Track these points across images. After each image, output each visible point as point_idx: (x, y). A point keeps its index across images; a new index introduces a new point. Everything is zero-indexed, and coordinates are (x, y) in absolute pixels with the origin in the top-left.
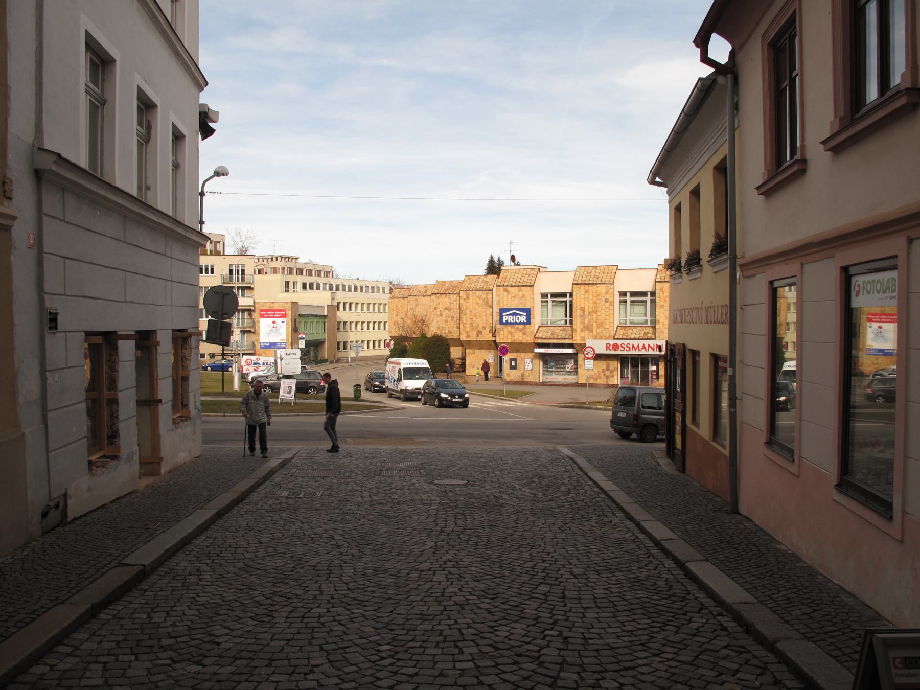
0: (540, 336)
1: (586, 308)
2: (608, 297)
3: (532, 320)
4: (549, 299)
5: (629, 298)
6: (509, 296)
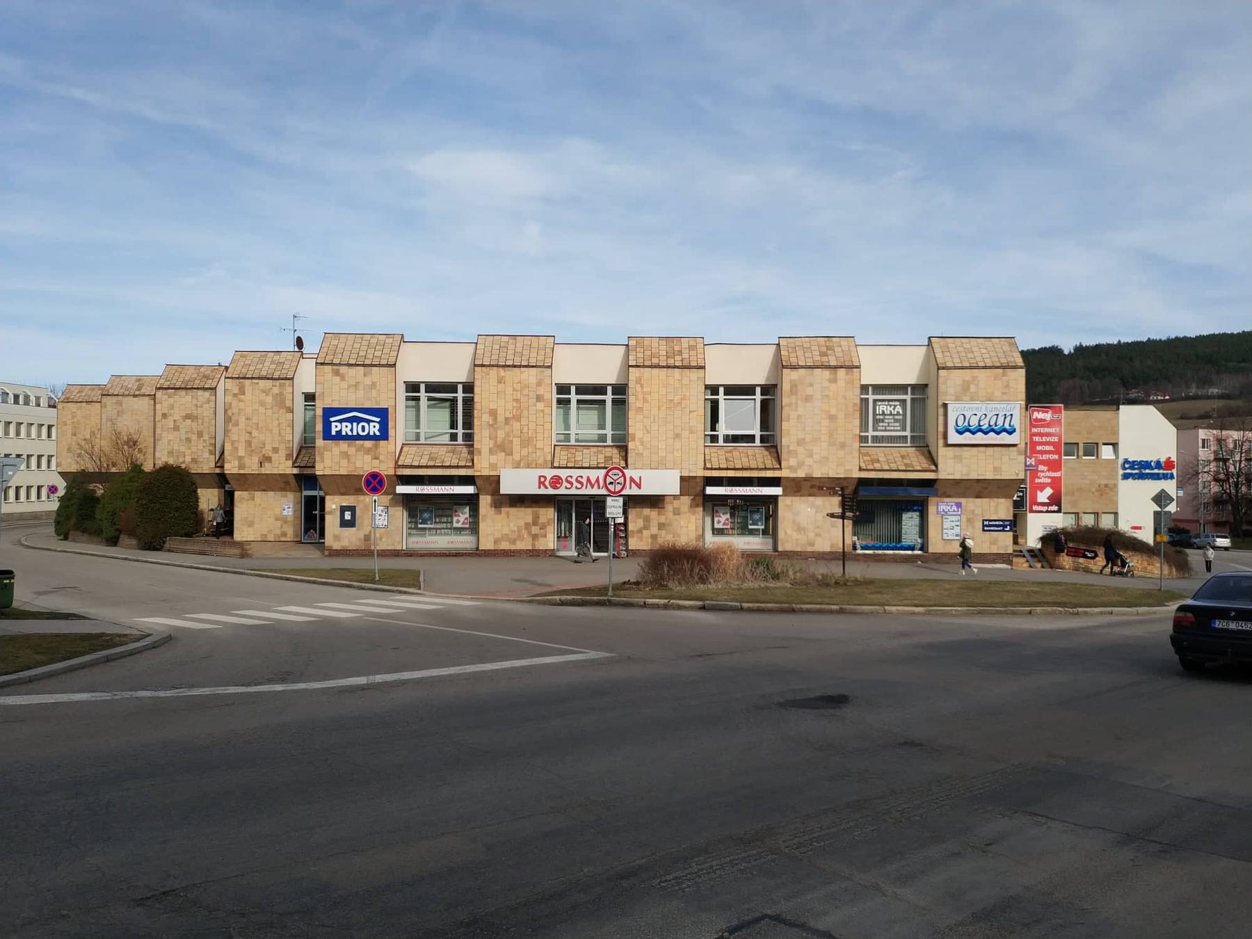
0: (408, 462)
1: (500, 412)
2: (541, 391)
3: (391, 432)
4: (423, 394)
5: (574, 397)
6: (344, 385)
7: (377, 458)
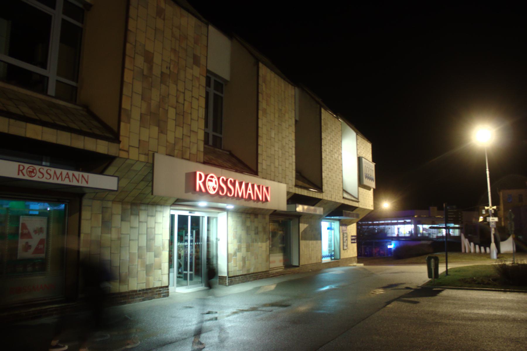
1: (157, 59)
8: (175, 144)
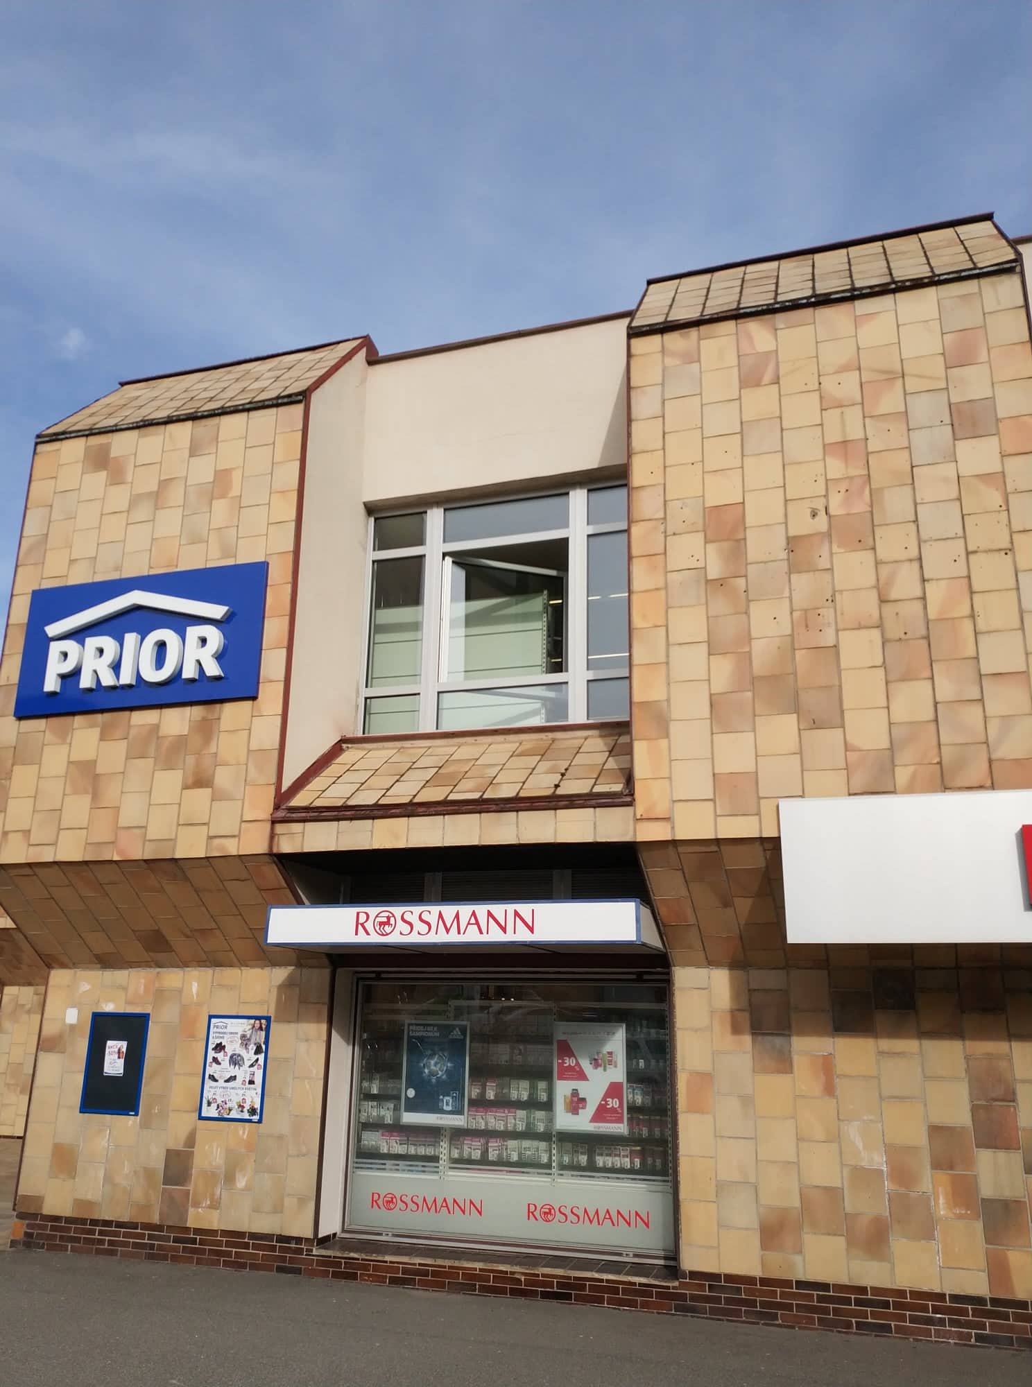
1: (763, 512)
3: (272, 663)
6: (119, 497)
7: (200, 781)
8: (891, 749)
